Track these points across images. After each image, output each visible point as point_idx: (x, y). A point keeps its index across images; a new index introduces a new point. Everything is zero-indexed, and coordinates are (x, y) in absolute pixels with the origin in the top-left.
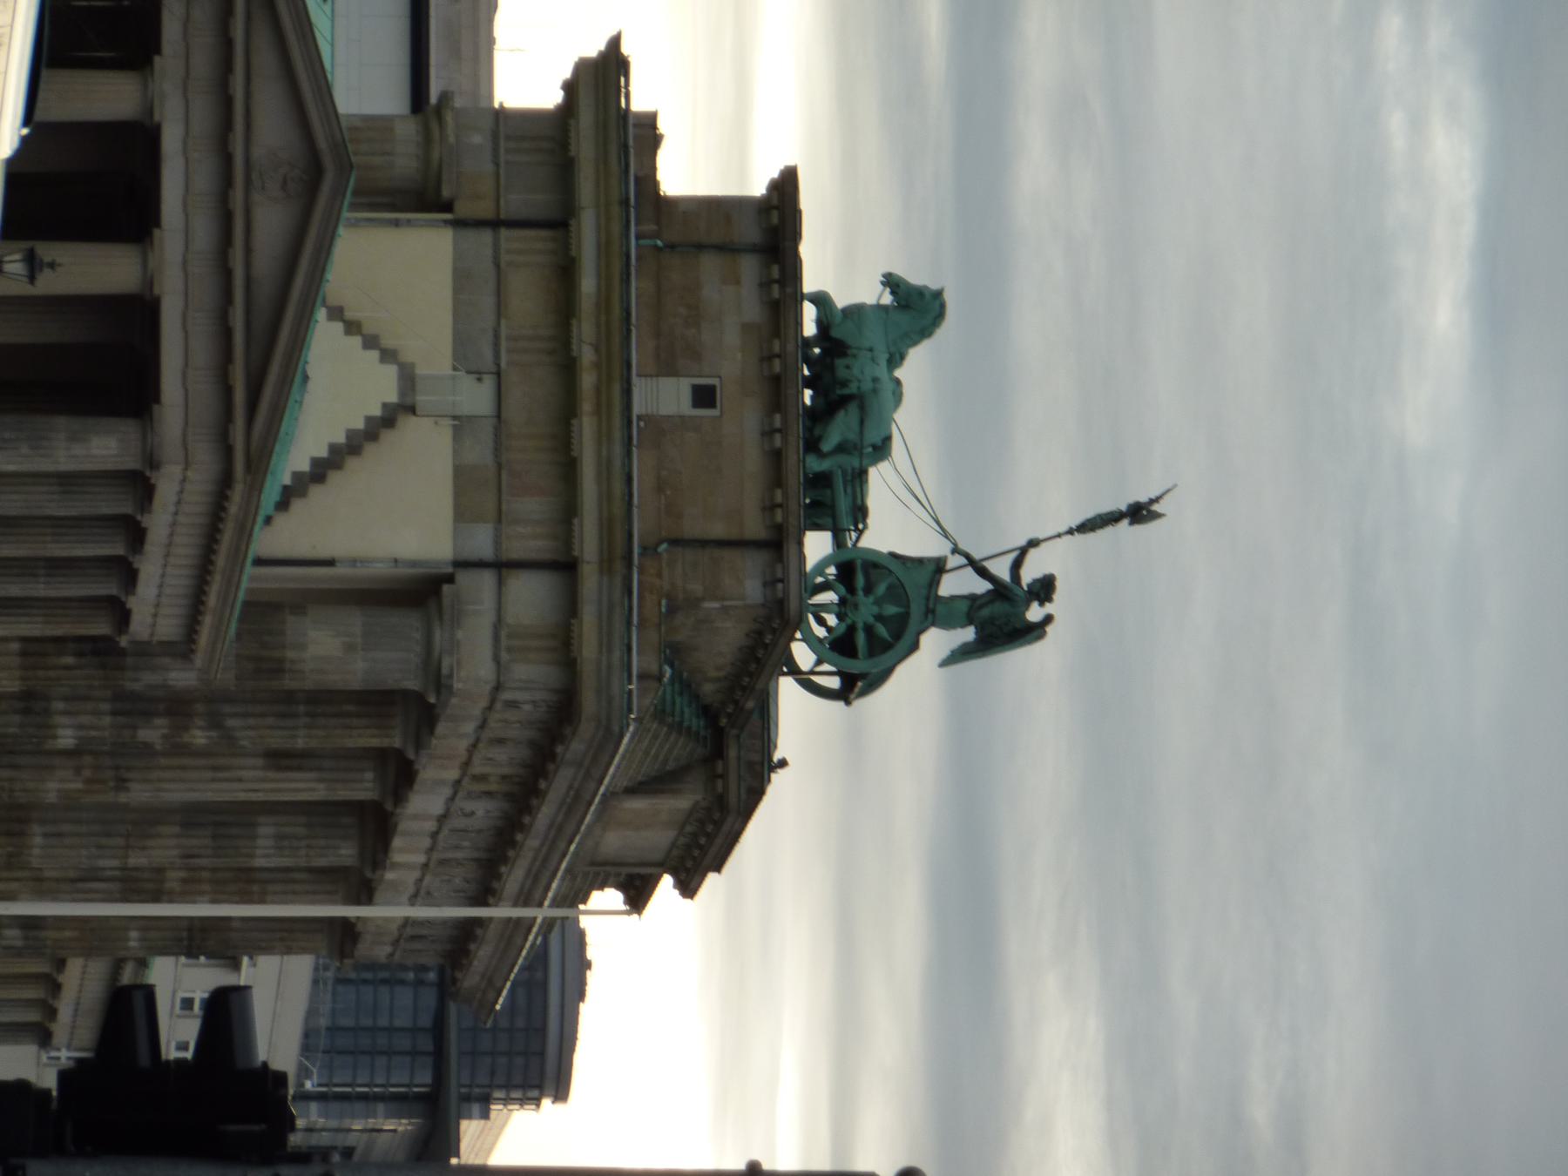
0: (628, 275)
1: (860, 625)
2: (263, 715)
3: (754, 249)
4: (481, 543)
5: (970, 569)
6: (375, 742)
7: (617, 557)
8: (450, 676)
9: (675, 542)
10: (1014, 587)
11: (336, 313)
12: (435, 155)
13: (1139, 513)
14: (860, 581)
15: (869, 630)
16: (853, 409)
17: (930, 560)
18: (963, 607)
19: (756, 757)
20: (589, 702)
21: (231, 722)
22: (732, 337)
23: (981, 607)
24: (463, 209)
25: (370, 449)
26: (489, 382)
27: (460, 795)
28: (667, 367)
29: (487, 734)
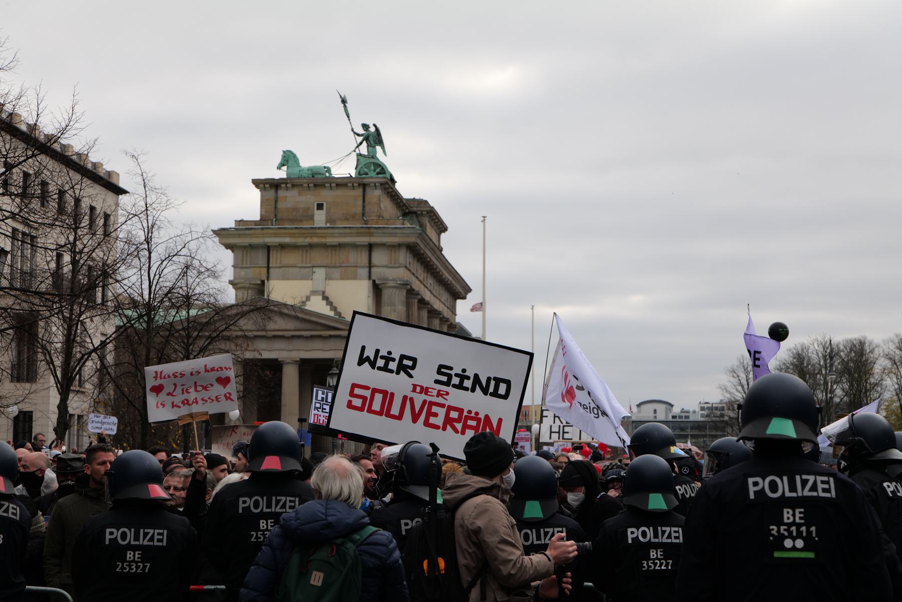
0: (284, 228)
3: (276, 191)
4: (364, 272)
5: (360, 147)
7: (368, 231)
8: (404, 281)
10: (365, 135)
12: (248, 285)
13: (344, 101)
17: (357, 157)
18: (370, 149)
24: (264, 277)
25: (335, 304)
26: (315, 270)
28: (311, 218)
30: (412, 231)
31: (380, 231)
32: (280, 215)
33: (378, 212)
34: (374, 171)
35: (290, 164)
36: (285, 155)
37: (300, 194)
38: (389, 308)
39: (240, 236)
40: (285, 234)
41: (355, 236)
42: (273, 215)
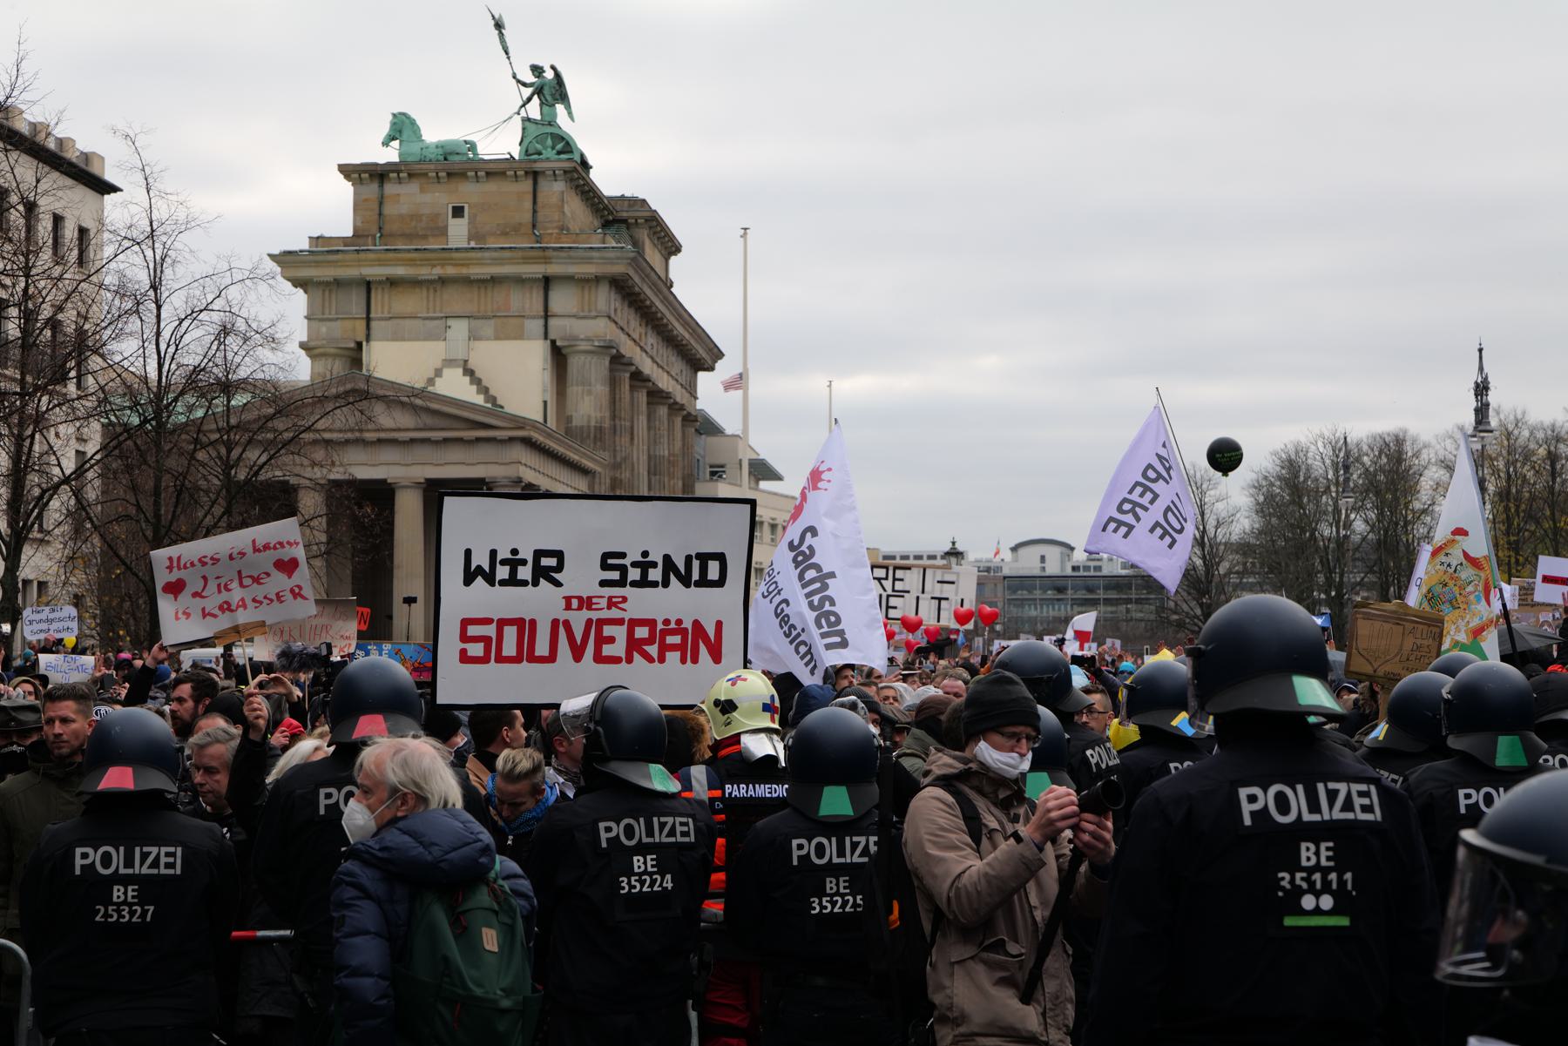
3: (381, 185)
4: (536, 325)
7: (543, 255)
8: (605, 341)
12: (332, 351)
13: (499, 26)
17: (523, 124)
18: (546, 108)
21: (618, 459)
22: (427, 198)
24: (361, 337)
25: (485, 383)
26: (450, 322)
28: (443, 232)
30: (619, 254)
31: (562, 254)
32: (387, 228)
35: (405, 137)
37: (422, 191)
38: (580, 388)
39: (318, 264)
40: (398, 260)
41: (518, 263)
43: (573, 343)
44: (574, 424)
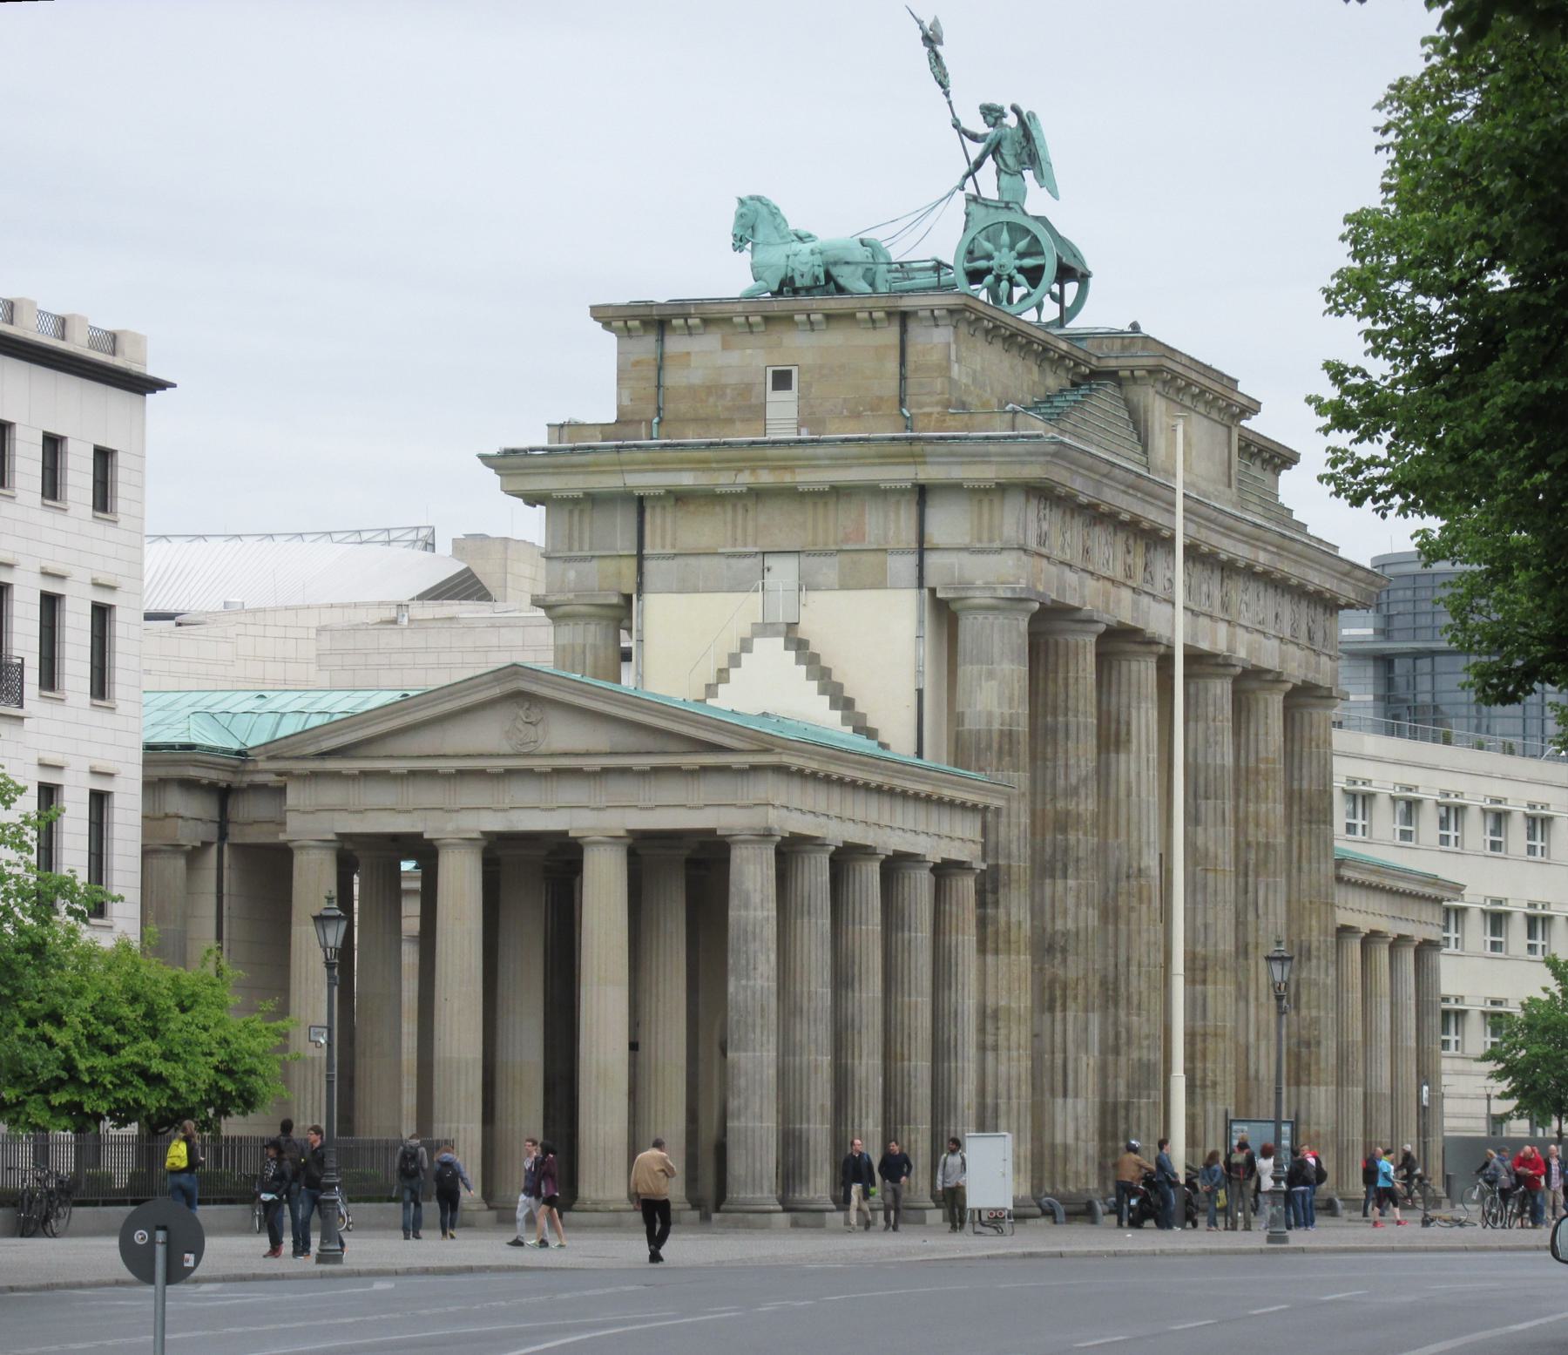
1: (1018, 263)
2: (1066, 751)
3: (661, 340)
4: (905, 565)
6: (1091, 658)
7: (911, 448)
8: (1013, 589)
9: (902, 403)
10: (988, 140)
11: (711, 690)
12: (583, 609)
13: (931, 40)
14: (982, 264)
15: (1021, 256)
16: (835, 271)
19: (1118, 343)
20: (1033, 472)
21: (1073, 780)
22: (734, 358)
23: (1006, 165)
24: (629, 587)
26: (770, 561)
27: (1147, 588)
29: (1078, 562)
30: (1030, 448)
31: (942, 449)
32: (670, 408)
33: (942, 393)
34: (1012, 248)
35: (760, 237)
36: (744, 210)
37: (726, 346)
38: (976, 668)
39: (558, 470)
40: (681, 461)
41: (874, 465)
42: (652, 408)
43: (963, 594)
44: (967, 727)
